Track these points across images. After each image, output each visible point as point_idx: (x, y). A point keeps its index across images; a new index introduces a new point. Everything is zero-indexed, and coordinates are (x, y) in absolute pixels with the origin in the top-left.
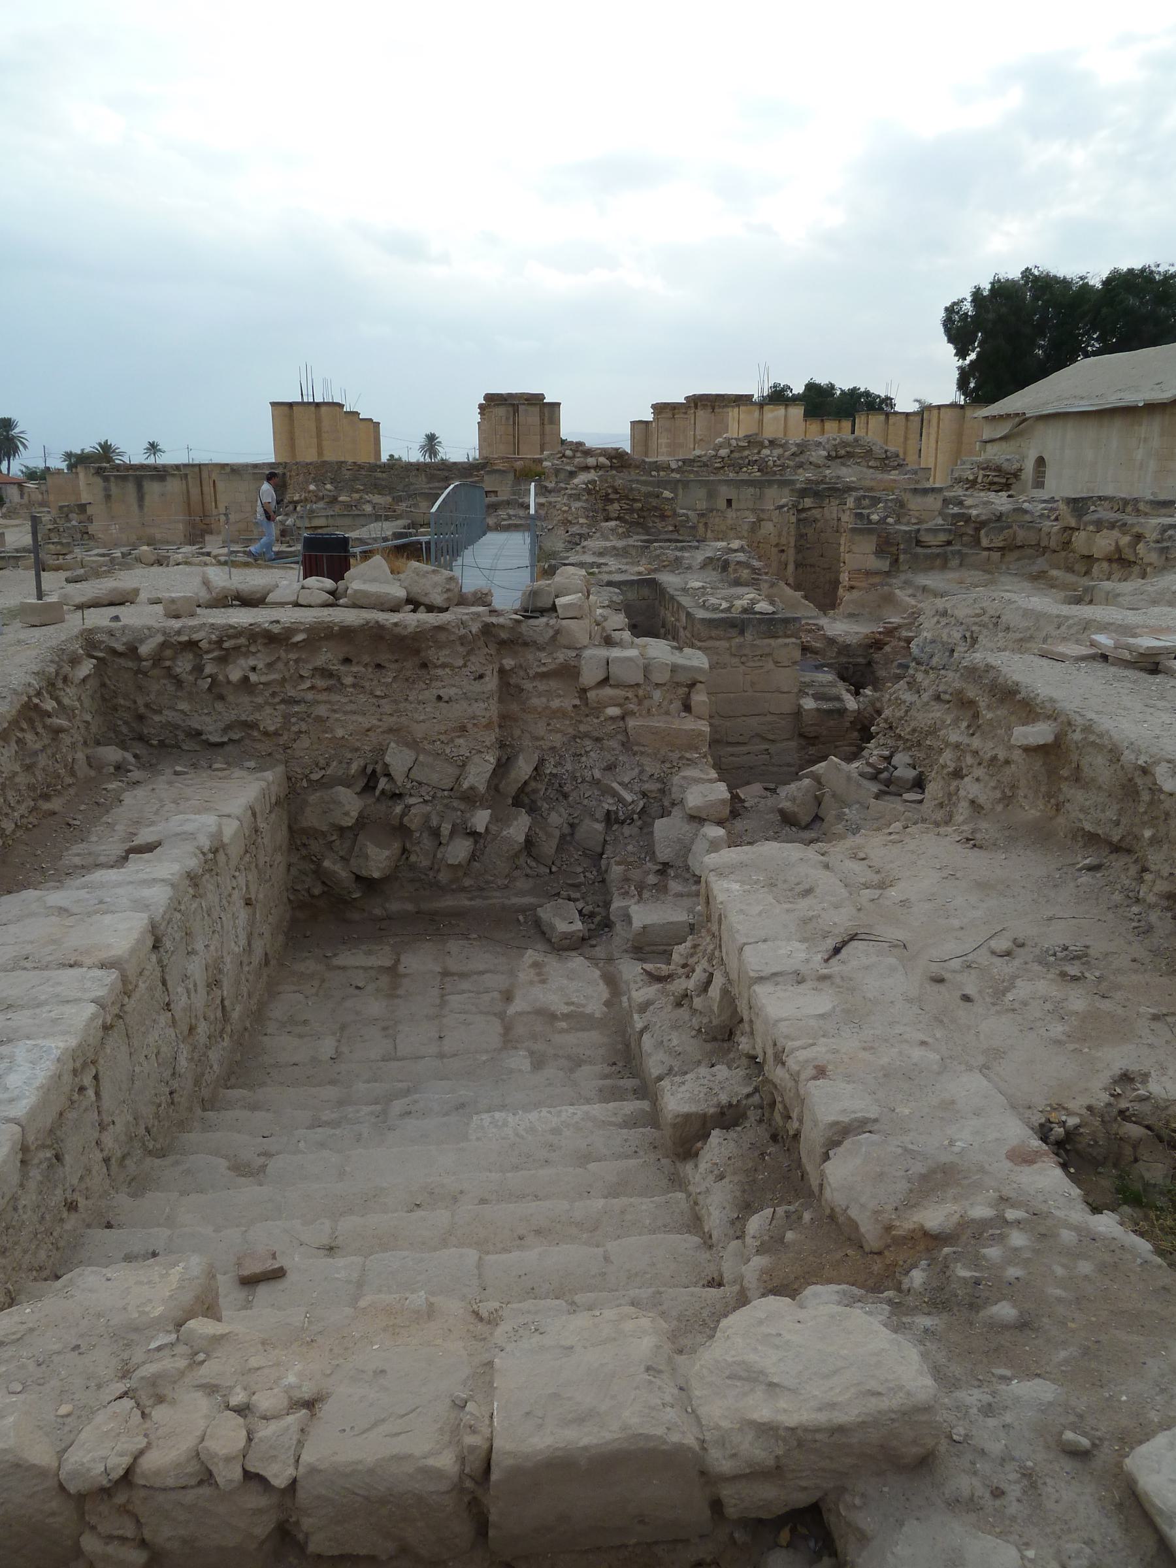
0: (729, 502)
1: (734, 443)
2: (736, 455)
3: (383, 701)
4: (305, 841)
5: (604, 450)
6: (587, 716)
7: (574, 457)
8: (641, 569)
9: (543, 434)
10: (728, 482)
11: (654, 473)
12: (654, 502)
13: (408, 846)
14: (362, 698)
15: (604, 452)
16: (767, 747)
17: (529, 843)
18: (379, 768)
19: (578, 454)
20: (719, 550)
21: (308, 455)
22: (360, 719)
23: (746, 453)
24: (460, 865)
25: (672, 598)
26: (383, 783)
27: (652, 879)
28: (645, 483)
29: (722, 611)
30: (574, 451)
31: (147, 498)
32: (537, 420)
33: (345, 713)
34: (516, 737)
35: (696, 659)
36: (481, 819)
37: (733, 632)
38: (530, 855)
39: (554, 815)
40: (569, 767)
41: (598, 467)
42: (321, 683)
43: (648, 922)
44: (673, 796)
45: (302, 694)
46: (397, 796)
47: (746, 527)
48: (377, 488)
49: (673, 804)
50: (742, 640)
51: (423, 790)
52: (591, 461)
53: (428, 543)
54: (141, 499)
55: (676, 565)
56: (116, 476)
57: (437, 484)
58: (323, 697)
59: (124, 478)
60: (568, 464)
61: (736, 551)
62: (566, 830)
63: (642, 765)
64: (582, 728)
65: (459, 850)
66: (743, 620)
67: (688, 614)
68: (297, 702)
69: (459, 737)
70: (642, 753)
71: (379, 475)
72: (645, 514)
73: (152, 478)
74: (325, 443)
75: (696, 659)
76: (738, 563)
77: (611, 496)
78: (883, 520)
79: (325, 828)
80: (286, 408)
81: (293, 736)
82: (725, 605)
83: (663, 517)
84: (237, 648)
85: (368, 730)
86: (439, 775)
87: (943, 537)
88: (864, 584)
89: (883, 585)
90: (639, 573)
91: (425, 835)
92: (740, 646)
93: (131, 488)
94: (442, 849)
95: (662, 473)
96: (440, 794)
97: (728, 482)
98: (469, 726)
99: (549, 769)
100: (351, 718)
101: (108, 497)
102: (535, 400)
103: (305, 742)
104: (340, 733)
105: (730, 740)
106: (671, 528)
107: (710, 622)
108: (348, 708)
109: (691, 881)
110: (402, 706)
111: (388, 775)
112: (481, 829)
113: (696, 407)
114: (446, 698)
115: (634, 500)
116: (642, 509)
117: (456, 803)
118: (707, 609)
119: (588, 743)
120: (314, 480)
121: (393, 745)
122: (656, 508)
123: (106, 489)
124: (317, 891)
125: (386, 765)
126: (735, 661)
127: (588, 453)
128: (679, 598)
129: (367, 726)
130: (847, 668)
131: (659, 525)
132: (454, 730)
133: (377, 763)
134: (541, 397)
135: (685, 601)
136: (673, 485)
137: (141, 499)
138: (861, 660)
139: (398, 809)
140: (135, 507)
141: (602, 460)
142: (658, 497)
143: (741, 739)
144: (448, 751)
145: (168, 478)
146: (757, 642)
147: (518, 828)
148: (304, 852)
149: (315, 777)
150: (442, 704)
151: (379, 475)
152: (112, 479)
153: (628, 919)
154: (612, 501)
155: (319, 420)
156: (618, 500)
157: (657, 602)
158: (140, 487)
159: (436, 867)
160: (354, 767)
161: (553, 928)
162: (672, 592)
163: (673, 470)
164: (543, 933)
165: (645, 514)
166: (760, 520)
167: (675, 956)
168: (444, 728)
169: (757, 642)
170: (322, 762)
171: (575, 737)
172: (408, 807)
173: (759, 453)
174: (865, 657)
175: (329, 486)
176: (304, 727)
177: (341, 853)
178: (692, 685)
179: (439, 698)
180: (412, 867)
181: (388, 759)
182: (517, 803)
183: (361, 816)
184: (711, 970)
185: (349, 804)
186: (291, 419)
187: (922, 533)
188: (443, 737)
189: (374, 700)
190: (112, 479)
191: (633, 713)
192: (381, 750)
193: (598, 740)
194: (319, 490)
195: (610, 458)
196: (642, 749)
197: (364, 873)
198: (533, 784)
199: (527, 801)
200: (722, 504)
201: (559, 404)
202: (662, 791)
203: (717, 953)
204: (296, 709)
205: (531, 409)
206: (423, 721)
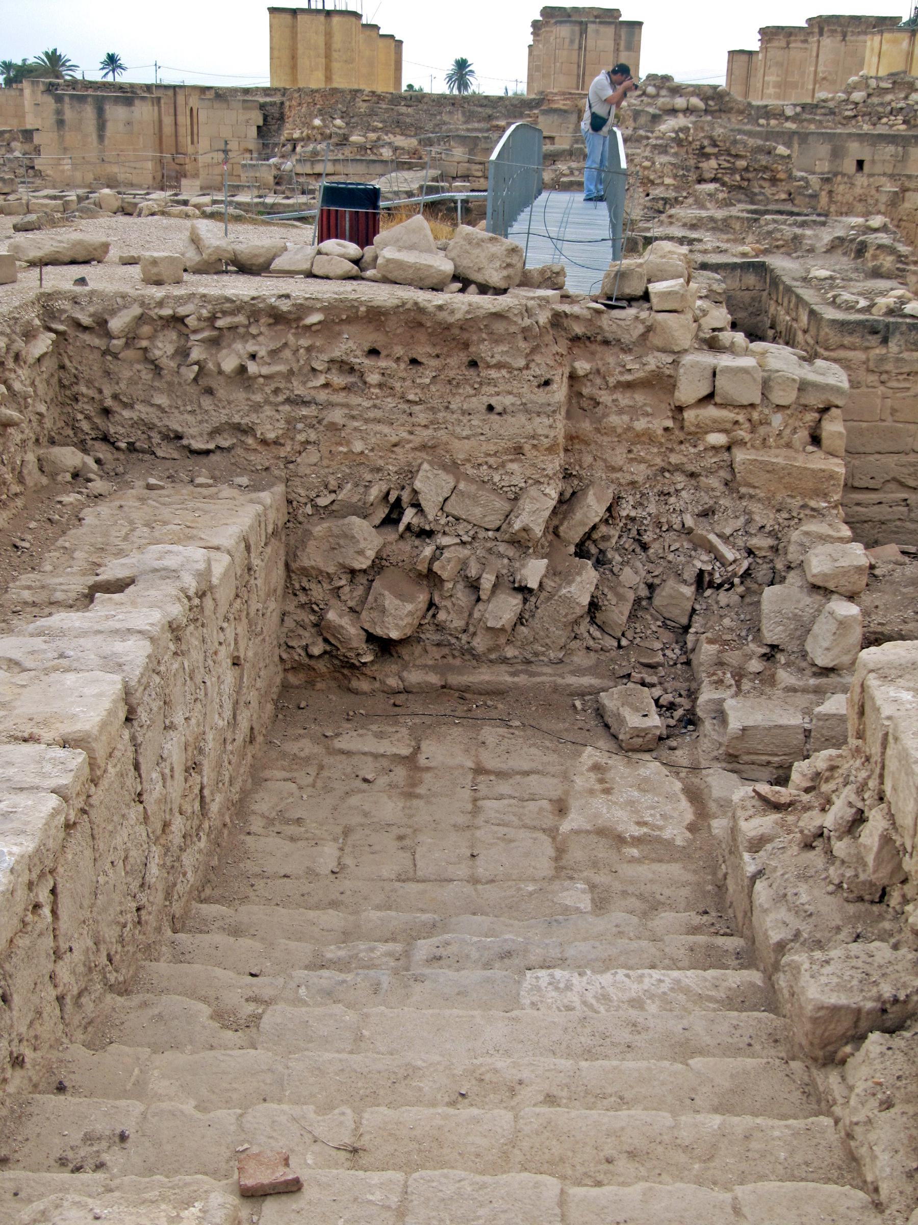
0: (860, 164)
1: (873, 83)
2: (875, 100)
3: (416, 409)
4: (305, 584)
5: (698, 87)
6: (681, 442)
7: (657, 95)
8: (747, 249)
10: (861, 137)
11: (762, 121)
12: (764, 160)
13: (437, 599)
14: (390, 402)
15: (698, 91)
16: (905, 496)
17: (594, 606)
18: (406, 496)
19: (663, 92)
20: (853, 228)
21: (316, 81)
22: (386, 429)
23: (889, 97)
24: (503, 629)
25: (789, 290)
26: (409, 516)
27: (755, 665)
28: (750, 134)
29: (860, 311)
30: (658, 88)
31: (110, 126)
32: (610, 44)
33: (367, 421)
34: (585, 465)
35: (831, 375)
36: (533, 571)
37: (874, 340)
38: (593, 621)
39: (627, 570)
40: (652, 508)
42: (338, 380)
43: (750, 723)
44: (790, 557)
45: (313, 392)
46: (426, 534)
47: (884, 198)
48: (399, 126)
49: (789, 568)
50: (884, 351)
51: (461, 528)
52: (680, 102)
53: (465, 202)
54: (101, 127)
55: (793, 246)
56: (72, 97)
57: (476, 125)
58: (340, 398)
59: (82, 99)
60: (649, 104)
61: (876, 230)
62: (644, 592)
63: (750, 513)
64: (674, 459)
65: (504, 609)
66: (887, 325)
67: (812, 313)
68: (306, 403)
69: (511, 461)
70: (752, 497)
71: (403, 109)
73: (117, 100)
75: (831, 375)
76: (880, 247)
77: (709, 150)
79: (331, 570)
80: (288, 17)
81: (298, 447)
82: (863, 303)
83: (774, 181)
84: (233, 328)
85: (395, 445)
86: (485, 510)
90: (744, 255)
91: (460, 586)
92: (882, 359)
93: (89, 111)
94: (480, 606)
95: (773, 122)
96: (482, 534)
97: (861, 137)
98: (527, 447)
99: (626, 510)
100: (376, 430)
101: (60, 123)
102: (609, 17)
103: (312, 456)
104: (358, 446)
105: (856, 484)
106: (784, 196)
107: (842, 326)
108: (371, 414)
109: (808, 672)
110: (441, 415)
111: (417, 505)
112: (533, 584)
113: (821, 34)
114: (499, 409)
115: (737, 156)
116: (746, 169)
117: (502, 548)
118: (839, 307)
119: (680, 478)
120: (321, 112)
121: (426, 466)
122: (766, 169)
123: (59, 112)
124: (316, 650)
125: (415, 492)
126: (872, 378)
127: (677, 90)
128: (800, 291)
129: (394, 439)
131: (768, 191)
132: (507, 451)
133: (403, 488)
135: (808, 294)
136: (788, 138)
137: (101, 127)
139: (428, 551)
140: (94, 137)
141: (695, 101)
142: (769, 153)
143: (871, 484)
144: (496, 478)
145: (137, 102)
146: (905, 355)
147: (583, 584)
148: (303, 599)
149: (323, 502)
150: (494, 417)
151: (403, 109)
152: (67, 99)
153: (721, 716)
154: (707, 156)
155: (329, 35)
156: (717, 156)
157: (765, 294)
158: (100, 112)
159: (472, 629)
160: (375, 493)
161: (621, 721)
162: (788, 282)
163: (787, 119)
164: (607, 726)
166: (905, 190)
167: (795, 776)
168: (494, 448)
169: (905, 355)
170: (333, 484)
171: (663, 470)
172: (440, 549)
173: (906, 98)
175: (338, 122)
176: (313, 437)
177: (351, 604)
178: (826, 410)
179: (490, 408)
180: (440, 628)
181: (418, 485)
182: (581, 552)
183: (379, 557)
184: (860, 805)
185: (366, 540)
186: (294, 29)
188: (491, 460)
189: (405, 406)
190: (67, 99)
191: (742, 443)
192: (411, 473)
193: (692, 475)
194: (325, 126)
195: (705, 99)
196: (751, 491)
197: (379, 631)
198: (603, 529)
199: (594, 550)
200: (849, 166)
202: (775, 549)
203: (872, 784)
204: (305, 411)
205: (603, 29)
206: (467, 438)
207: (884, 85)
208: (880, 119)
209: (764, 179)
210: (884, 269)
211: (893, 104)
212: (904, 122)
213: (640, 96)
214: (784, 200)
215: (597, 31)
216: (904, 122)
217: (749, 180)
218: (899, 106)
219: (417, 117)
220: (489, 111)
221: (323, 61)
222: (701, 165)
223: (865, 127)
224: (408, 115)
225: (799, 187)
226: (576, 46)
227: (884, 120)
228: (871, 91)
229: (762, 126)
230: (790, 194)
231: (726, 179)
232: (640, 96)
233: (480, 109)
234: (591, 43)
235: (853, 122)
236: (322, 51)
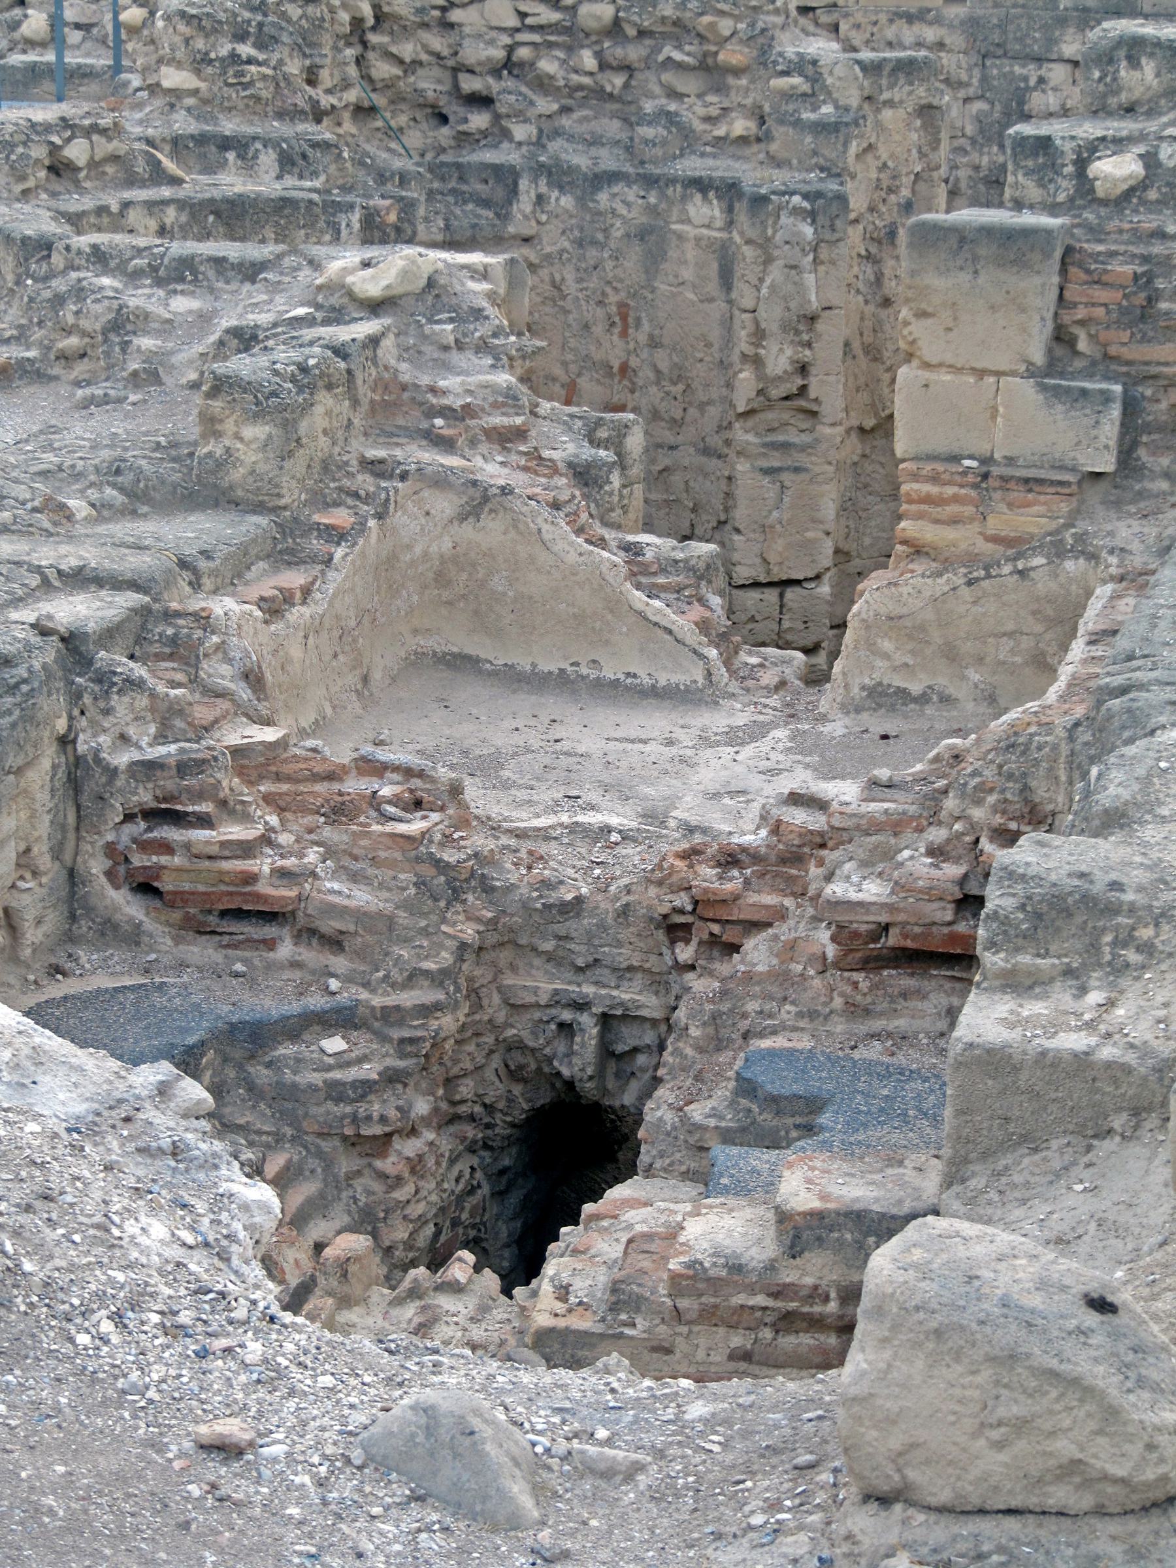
72: (634, 53)
83: (711, 70)
88: (963, 538)
89: (1058, 551)
106: (741, 126)
116: (615, 29)
130: (566, 1028)
138: (632, 994)
165: (634, 53)
174: (658, 982)
209: (680, 66)
210: (237, 474)
214: (743, 140)
217: (627, 68)
222: (456, 15)
225: (789, 95)
230: (762, 121)
231: (548, 66)
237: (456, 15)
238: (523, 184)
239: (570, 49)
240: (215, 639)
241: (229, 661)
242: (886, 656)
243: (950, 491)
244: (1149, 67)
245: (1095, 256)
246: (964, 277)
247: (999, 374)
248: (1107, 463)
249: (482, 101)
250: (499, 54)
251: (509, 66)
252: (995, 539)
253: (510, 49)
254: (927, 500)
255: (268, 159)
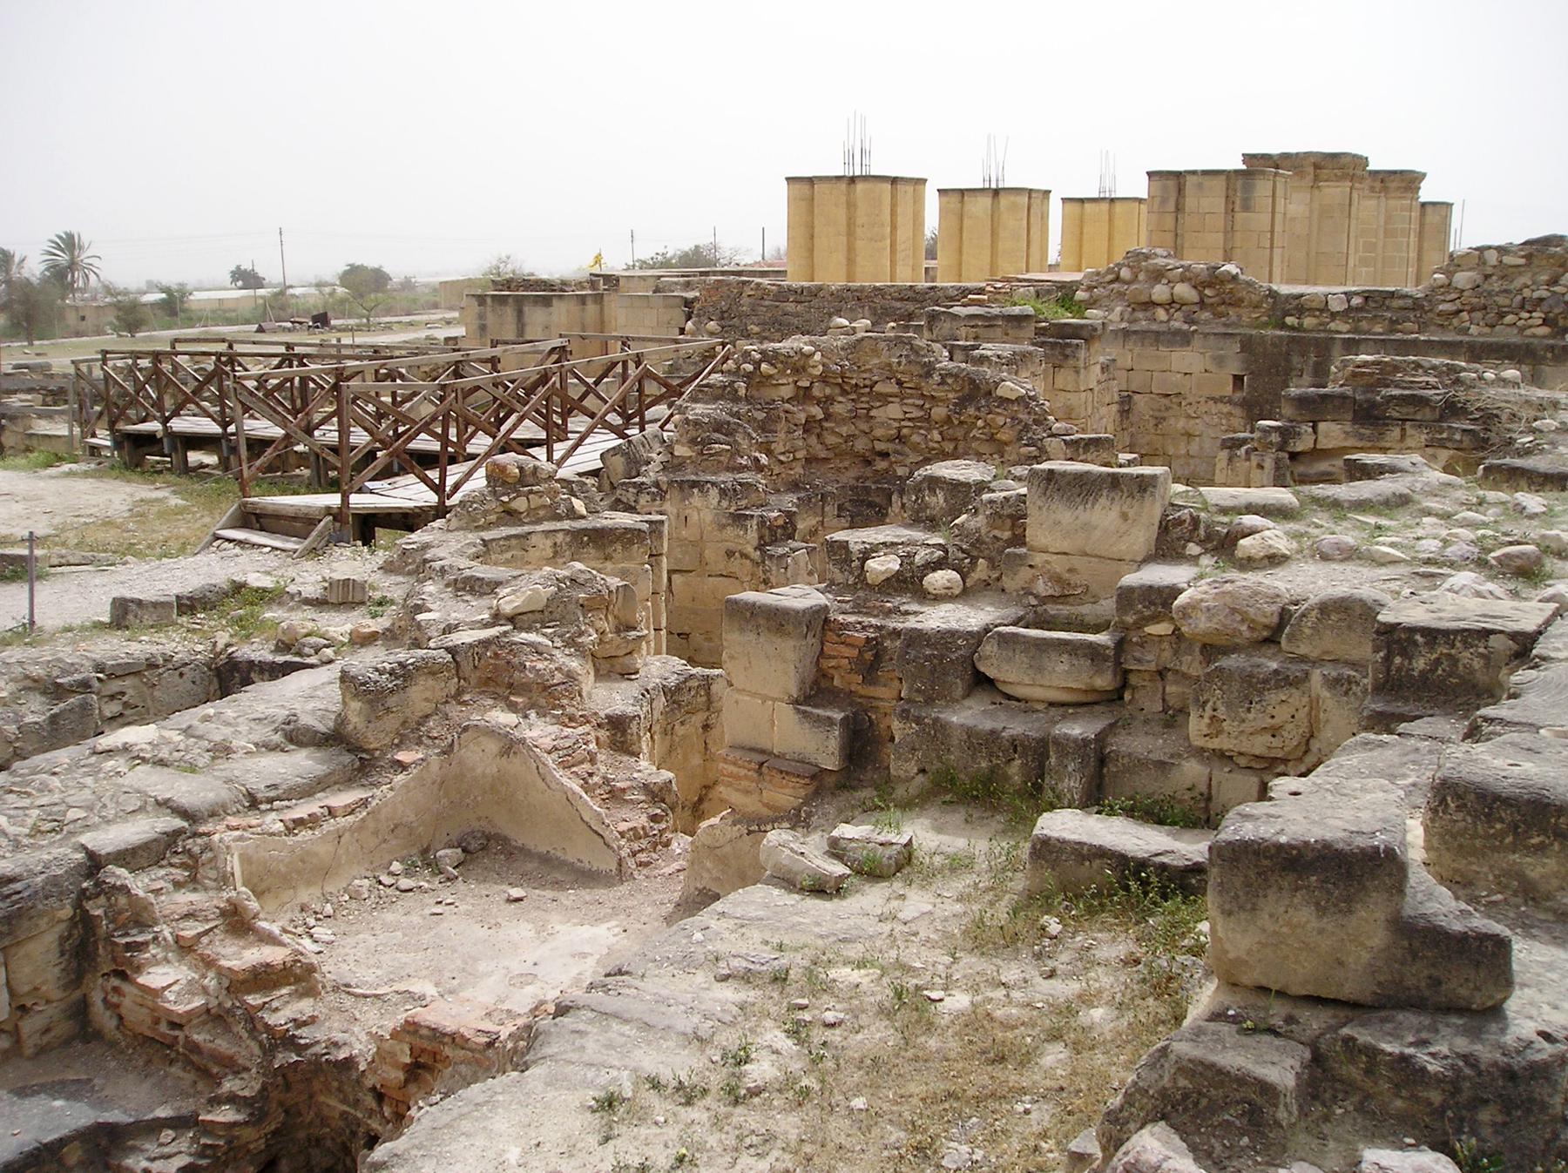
1: (1492, 258)
7: (1134, 280)
9: (1230, 230)
23: (1525, 279)
32: (1219, 204)
41: (1172, 303)
52: (1160, 292)
71: (790, 307)
72: (959, 433)
73: (538, 301)
74: (859, 244)
78: (909, 582)
80: (805, 187)
87: (1063, 678)
93: (509, 312)
123: (481, 316)
134: (1361, 161)
141: (1184, 291)
145: (555, 301)
154: (885, 399)
155: (851, 205)
158: (520, 313)
163: (1334, 315)
187: (989, 648)
190: (489, 300)
195: (1199, 286)
201: (1424, 175)
207: (1507, 260)
208: (1502, 315)
211: (1527, 293)
212: (1545, 322)
213: (1112, 282)
215: (1200, 186)
216: (1545, 322)
218: (1536, 295)
219: (807, 317)
220: (911, 307)
221: (844, 239)
222: (873, 413)
223: (1474, 329)
224: (797, 315)
226: (1171, 206)
227: (1509, 319)
228: (1489, 271)
229: (1292, 328)
231: (915, 438)
232: (1112, 282)
233: (898, 304)
234: (1190, 202)
235: (1455, 322)
236: (843, 229)
237: (873, 413)
238: (894, 497)
239: (929, 430)
240: (210, 855)
241: (216, 868)
242: (708, 871)
243: (743, 772)
244: (941, 496)
245: (845, 626)
246: (752, 636)
247: (774, 700)
248: (831, 762)
249: (885, 455)
250: (894, 432)
251: (899, 437)
252: (767, 805)
253: (899, 429)
254: (731, 775)
255: (714, 492)
